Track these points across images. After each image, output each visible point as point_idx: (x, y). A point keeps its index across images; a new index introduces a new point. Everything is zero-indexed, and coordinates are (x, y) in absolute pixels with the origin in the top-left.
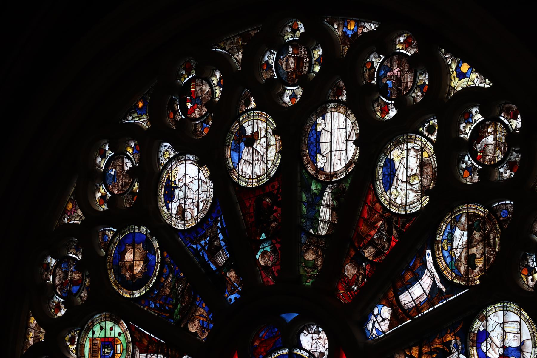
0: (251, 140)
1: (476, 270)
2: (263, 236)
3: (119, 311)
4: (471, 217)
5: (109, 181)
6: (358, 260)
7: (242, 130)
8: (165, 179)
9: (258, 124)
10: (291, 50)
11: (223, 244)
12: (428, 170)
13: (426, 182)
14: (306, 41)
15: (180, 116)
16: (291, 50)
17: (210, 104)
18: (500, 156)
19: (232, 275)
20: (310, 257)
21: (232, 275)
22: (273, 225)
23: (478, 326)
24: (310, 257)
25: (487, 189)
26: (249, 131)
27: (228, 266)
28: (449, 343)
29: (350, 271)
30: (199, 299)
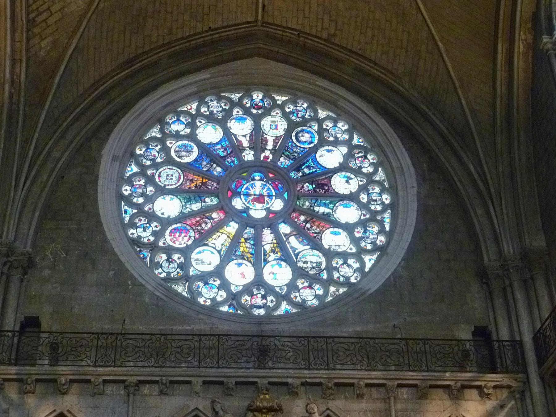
0: (347, 182)
1: (302, 264)
2: (314, 186)
3: (288, 132)
4: (321, 263)
5: (334, 128)
6: (306, 221)
7: (351, 179)
8: (334, 149)
9: (354, 185)
10: (380, 198)
11: (311, 171)
12: (337, 247)
13: (333, 247)
14: (383, 203)
15: (356, 156)
16: (380, 198)
17: (360, 168)
18: (342, 274)
19: (300, 174)
20: (307, 203)
21: (300, 174)
22: (318, 190)
23: (283, 264)
24: (307, 203)
25: (330, 269)
26: (350, 181)
27: (304, 173)
28: (277, 253)
29: (302, 218)
30: (292, 162)
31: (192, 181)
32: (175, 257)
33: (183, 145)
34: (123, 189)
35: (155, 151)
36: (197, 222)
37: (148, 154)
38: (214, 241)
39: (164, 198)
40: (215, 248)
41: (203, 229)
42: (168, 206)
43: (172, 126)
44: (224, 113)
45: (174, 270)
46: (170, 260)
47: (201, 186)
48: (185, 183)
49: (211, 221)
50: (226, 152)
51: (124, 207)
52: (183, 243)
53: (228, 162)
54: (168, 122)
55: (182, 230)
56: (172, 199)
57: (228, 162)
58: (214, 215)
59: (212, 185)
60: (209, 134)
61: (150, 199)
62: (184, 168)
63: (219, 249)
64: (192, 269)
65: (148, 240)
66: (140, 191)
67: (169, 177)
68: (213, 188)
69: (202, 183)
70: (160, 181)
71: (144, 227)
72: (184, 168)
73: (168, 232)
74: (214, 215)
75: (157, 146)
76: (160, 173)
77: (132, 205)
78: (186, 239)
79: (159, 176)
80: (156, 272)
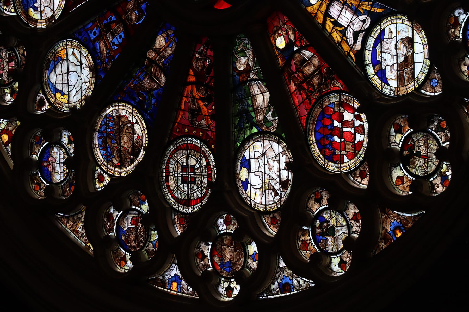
31: (196, 113)
32: (397, 139)
33: (104, 146)
34: (226, 299)
35: (124, 221)
36: (299, 88)
37: (132, 237)
38: (350, 35)
39: (246, 183)
40: (368, 33)
41: (318, 69)
42: (265, 170)
43: (57, 178)
44: (14, 42)
45: (432, 142)
46: (406, 153)
47: (207, 87)
48: (203, 131)
49: (296, 48)
50: (113, 26)
51: (275, 292)
52: (357, 123)
53: (138, 19)
54: (47, 190)
55: (325, 126)
56: (247, 164)
57: (138, 19)
58: (281, 43)
59: (202, 59)
60: (72, 77)
61: (249, 221)
62: (163, 138)
63: (369, 21)
64: (426, 92)
65: (355, 218)
66: (228, 254)
67: (186, 178)
68: (209, 53)
69: (197, 84)
70: (201, 199)
71: (323, 234)
72: (163, 138)
73: (332, 167)
74: (281, 43)
75: (110, 216)
76: (178, 200)
77: (266, 270)
78: (348, 116)
79: (188, 202)
80: (440, 189)
